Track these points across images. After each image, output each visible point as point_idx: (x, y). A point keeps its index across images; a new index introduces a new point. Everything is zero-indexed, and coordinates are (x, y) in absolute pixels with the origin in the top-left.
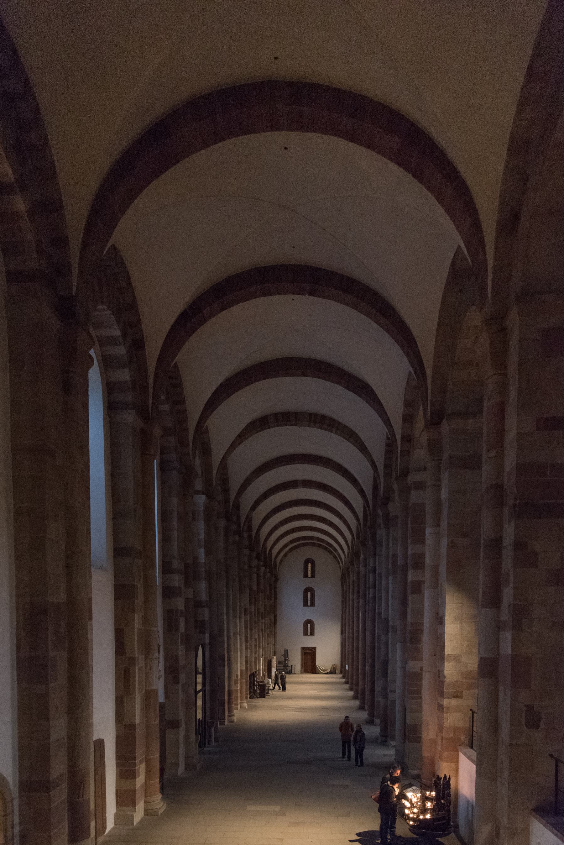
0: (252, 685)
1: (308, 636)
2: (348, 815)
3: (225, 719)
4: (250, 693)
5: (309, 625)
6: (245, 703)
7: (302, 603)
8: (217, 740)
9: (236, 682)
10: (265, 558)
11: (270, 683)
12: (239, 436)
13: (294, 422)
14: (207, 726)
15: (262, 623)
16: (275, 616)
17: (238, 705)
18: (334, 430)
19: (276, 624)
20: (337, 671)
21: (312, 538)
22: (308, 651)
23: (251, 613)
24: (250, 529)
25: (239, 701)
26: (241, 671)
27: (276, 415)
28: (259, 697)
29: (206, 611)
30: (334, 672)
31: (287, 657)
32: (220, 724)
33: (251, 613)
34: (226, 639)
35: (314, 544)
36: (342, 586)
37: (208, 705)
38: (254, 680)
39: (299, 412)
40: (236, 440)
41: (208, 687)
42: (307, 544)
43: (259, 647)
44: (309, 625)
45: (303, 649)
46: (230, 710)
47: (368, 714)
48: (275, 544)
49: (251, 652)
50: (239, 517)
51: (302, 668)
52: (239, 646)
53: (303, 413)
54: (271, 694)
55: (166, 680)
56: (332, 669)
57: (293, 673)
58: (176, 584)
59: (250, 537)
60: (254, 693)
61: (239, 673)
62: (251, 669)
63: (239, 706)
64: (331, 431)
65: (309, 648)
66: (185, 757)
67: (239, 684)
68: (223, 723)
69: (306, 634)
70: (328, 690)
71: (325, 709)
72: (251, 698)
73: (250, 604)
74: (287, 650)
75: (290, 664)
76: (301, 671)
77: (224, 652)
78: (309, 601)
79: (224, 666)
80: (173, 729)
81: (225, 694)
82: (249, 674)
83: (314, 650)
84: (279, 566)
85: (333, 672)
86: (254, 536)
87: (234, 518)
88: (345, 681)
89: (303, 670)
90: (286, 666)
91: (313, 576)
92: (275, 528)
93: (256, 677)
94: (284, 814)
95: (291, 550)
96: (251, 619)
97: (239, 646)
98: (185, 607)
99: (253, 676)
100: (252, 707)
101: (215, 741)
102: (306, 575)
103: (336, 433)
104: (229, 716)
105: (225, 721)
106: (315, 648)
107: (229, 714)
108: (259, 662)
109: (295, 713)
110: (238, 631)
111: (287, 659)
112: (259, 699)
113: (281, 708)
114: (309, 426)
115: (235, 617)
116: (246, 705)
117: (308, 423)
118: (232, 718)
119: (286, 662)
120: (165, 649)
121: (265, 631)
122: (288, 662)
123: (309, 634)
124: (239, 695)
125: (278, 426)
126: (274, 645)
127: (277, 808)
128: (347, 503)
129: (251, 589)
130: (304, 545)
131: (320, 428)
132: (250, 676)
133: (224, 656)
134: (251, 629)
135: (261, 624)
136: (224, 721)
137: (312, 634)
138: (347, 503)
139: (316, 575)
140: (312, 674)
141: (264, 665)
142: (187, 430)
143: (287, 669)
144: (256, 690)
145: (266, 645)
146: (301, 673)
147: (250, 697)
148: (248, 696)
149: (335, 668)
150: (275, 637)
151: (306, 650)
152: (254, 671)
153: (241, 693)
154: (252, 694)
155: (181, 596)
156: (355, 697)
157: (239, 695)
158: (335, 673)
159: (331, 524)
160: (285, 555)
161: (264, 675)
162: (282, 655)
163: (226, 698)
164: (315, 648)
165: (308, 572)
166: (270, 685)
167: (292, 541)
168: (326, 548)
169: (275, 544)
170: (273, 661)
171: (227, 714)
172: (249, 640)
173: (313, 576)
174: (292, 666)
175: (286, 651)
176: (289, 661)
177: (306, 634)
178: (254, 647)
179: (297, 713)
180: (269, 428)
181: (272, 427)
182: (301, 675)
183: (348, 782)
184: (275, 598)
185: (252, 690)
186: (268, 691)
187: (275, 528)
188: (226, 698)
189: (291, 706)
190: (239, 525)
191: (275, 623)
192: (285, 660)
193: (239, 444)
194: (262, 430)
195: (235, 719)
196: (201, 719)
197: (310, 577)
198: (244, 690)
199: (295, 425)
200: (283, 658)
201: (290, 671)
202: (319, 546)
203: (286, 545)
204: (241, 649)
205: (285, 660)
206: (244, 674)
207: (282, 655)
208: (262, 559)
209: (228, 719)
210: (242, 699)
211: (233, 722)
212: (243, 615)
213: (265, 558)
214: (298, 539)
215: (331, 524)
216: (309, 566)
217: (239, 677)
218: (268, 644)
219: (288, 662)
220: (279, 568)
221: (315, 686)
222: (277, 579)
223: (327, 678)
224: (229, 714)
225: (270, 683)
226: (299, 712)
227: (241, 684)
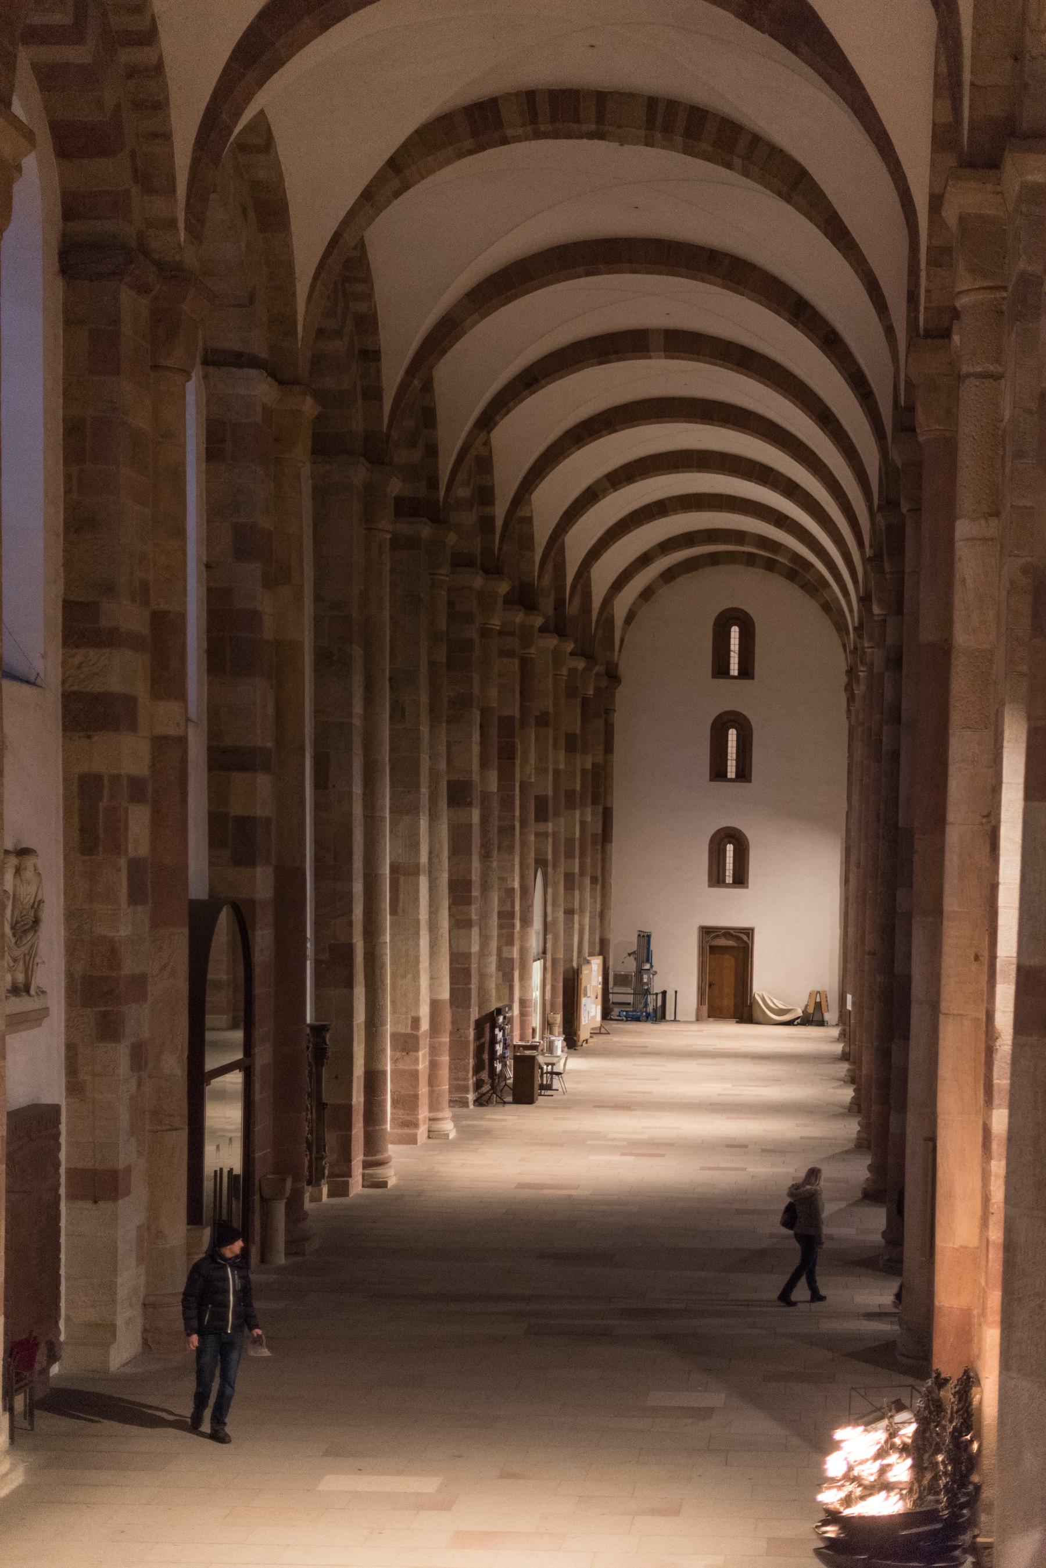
0: (486, 1056)
1: (728, 886)
2: (674, 1511)
3: (349, 1174)
4: (478, 1085)
5: (730, 848)
6: (447, 1118)
7: (704, 767)
8: (294, 1245)
9: (407, 1044)
10: (560, 604)
11: (559, 1052)
12: (394, 164)
13: (593, 127)
14: (257, 1197)
15: (541, 835)
16: (607, 815)
17: (415, 1125)
18: (737, 161)
19: (611, 842)
20: (827, 1016)
21: (739, 536)
22: (723, 942)
23: (485, 797)
24: (485, 495)
25: (423, 1113)
26: (434, 1004)
27: (530, 97)
28: (510, 1099)
29: (263, 782)
30: (815, 1019)
31: (648, 959)
32: (331, 1194)
33: (485, 797)
34: (358, 887)
35: (750, 560)
36: (849, 711)
37: (263, 1124)
38: (493, 1041)
39: (611, 93)
40: (379, 180)
41: (263, 1056)
42: (730, 558)
43: (526, 922)
44: (730, 848)
45: (707, 932)
46: (373, 1143)
47: (871, 1168)
48: (595, 553)
49: (485, 939)
50: (432, 451)
51: (701, 1001)
52: (423, 915)
53: (627, 97)
54: (560, 1089)
55: (71, 1024)
56: (811, 1010)
57: (668, 1018)
58: (115, 684)
59: (486, 523)
60: (493, 1087)
61: (424, 1012)
62: (483, 1001)
63: (422, 1131)
64: (729, 166)
65: (727, 932)
66: (144, 1305)
67: (421, 1053)
68: (340, 1189)
69: (716, 879)
70: (776, 1081)
71: (736, 1146)
72: (480, 1102)
73: (484, 764)
74: (649, 937)
75: (657, 988)
76: (698, 1010)
77: (350, 935)
78: (729, 763)
79: (350, 984)
80: (96, 1202)
81: (350, 1082)
82: (475, 1014)
83: (745, 938)
84: (624, 630)
85: (812, 1018)
86: (499, 523)
87: (403, 456)
88: (843, 1052)
89: (705, 1008)
90: (643, 991)
91: (746, 671)
92: (590, 497)
93: (502, 1029)
94: (445, 1506)
95: (669, 575)
96: (484, 821)
97: (423, 915)
98: (153, 765)
99: (489, 1022)
100: (470, 1135)
101: (287, 1254)
102: (721, 670)
103: (746, 174)
104: (366, 1165)
105: (352, 1181)
106: (749, 932)
107: (370, 1158)
108: (525, 975)
109: (623, 1158)
110: (424, 859)
111: (647, 966)
112: (508, 1107)
113: (578, 1142)
114: (649, 143)
115: (404, 809)
116: (448, 1127)
117: (643, 133)
118: (379, 1171)
119: (642, 979)
120: (72, 915)
121: (555, 866)
122: (649, 979)
123: (729, 879)
124: (423, 1090)
125: (538, 135)
126: (602, 915)
127: (427, 1485)
128: (825, 418)
129: (485, 712)
130: (714, 559)
131: (688, 151)
132: (479, 1025)
133: (350, 948)
134: (486, 856)
135: (532, 838)
136: (346, 1184)
137: (741, 879)
138: (825, 418)
139: (757, 670)
140: (737, 1022)
141: (548, 987)
142: (165, 137)
143: (646, 1005)
144: (502, 1076)
145: (561, 915)
146: (699, 1019)
147: (475, 1101)
148: (471, 1097)
149: (818, 1006)
150: (603, 887)
151: (716, 937)
152: (494, 1006)
153: (432, 1081)
154: (486, 1088)
155: (133, 727)
156: (856, 1107)
157: (423, 1090)
158: (821, 1023)
159: (790, 489)
160: (647, 594)
161: (548, 1025)
162: (629, 955)
163: (358, 1098)
164: (749, 932)
165: (729, 657)
166: (555, 1060)
167: (666, 546)
168: (792, 575)
169: (595, 553)
170: (585, 971)
171: (358, 1158)
172: (476, 893)
173: (746, 671)
174: (664, 993)
175: (645, 938)
176: (655, 973)
177: (716, 879)
178: (494, 921)
179: (631, 1158)
180: (504, 141)
181: (517, 139)
182: (696, 1027)
183: (716, 1398)
184: (609, 749)
185: (485, 1075)
186: (552, 1079)
187: (590, 497)
188: (358, 1098)
189: (614, 1136)
190: (433, 483)
191: (605, 837)
192: (640, 972)
193: (397, 194)
194: (480, 148)
195: (392, 1176)
196: (238, 1170)
197: (734, 677)
198: (444, 1073)
199: (601, 136)
200: (630, 966)
201: (655, 1010)
202: (770, 566)
203: (645, 559)
204: (433, 927)
205: (640, 972)
206: (447, 1015)
207: (629, 955)
208: (547, 605)
209: (364, 1175)
210: (434, 1106)
211: (384, 1185)
212: (443, 803)
213: (560, 604)
214: (688, 539)
215: (790, 489)
216: (733, 635)
217: (425, 1026)
218: (569, 912)
219: (649, 979)
220: (622, 641)
221: (730, 1067)
222: (613, 676)
223: (790, 1038)
224: (370, 1158)
225: (559, 1052)
226: (638, 1155)
227: (434, 1050)
